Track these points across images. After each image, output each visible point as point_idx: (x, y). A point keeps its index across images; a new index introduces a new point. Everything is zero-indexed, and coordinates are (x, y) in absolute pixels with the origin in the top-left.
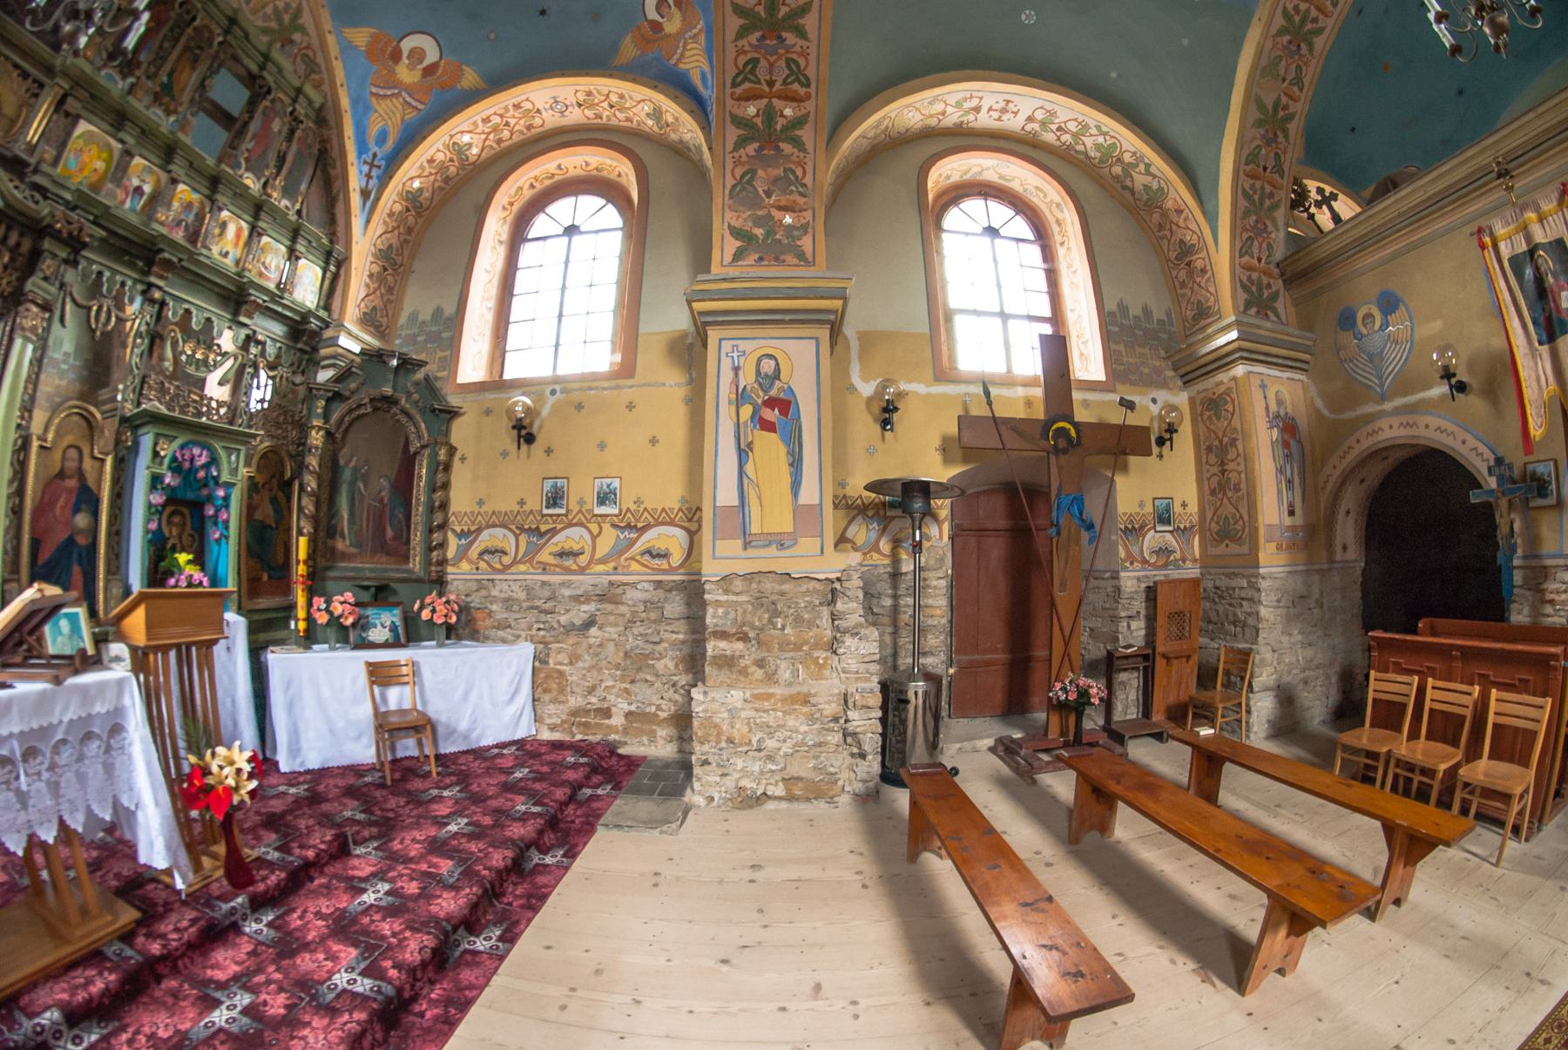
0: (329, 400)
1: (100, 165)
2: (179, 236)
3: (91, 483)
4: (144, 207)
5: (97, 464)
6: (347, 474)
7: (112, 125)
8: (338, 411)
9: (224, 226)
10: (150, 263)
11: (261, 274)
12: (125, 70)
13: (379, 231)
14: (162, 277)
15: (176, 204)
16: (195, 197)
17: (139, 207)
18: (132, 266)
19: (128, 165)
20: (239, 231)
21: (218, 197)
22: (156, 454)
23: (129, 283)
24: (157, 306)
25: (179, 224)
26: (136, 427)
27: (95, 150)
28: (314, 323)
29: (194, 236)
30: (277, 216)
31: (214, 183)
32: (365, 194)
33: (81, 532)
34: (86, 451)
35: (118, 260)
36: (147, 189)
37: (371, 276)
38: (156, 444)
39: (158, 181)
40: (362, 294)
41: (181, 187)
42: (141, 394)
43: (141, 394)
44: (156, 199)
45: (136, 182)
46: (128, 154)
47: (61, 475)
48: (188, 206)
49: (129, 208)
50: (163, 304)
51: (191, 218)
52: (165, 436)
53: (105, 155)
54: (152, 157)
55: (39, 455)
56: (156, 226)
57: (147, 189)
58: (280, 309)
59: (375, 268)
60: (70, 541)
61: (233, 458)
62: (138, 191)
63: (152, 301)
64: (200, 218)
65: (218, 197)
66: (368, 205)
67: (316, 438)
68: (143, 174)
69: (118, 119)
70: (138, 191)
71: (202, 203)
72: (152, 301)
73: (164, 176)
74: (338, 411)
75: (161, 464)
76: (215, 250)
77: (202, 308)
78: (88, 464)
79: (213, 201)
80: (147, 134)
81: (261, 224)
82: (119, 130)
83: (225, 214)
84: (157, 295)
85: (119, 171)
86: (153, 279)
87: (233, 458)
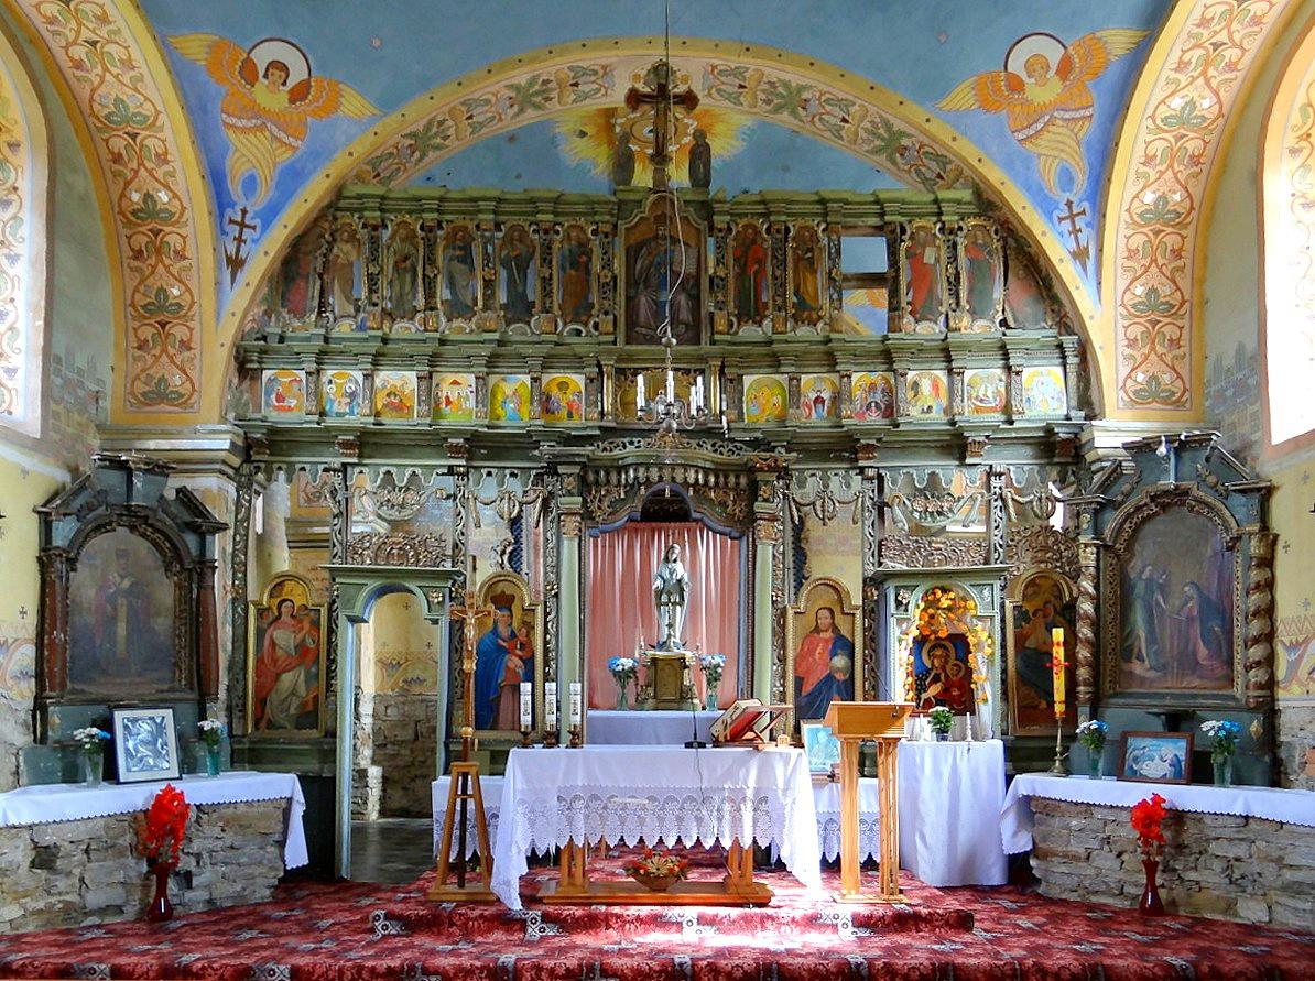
0: (1096, 513)
1: (778, 400)
2: (874, 419)
3: (845, 632)
4: (829, 413)
5: (850, 617)
6: (1140, 589)
7: (770, 366)
8: (1111, 521)
9: (916, 385)
10: (856, 452)
11: (978, 410)
12: (758, 318)
13: (1122, 285)
14: (869, 458)
15: (858, 393)
16: (874, 376)
17: (825, 414)
18: (841, 459)
19: (798, 386)
20: (936, 387)
21: (895, 366)
22: (898, 603)
23: (842, 473)
24: (875, 481)
25: (868, 407)
26: (882, 583)
27: (767, 391)
28: (1063, 434)
29: (890, 411)
30: (975, 348)
31: (887, 357)
32: (1079, 255)
33: (838, 670)
34: (837, 610)
35: (829, 460)
36: (826, 395)
37: (1132, 343)
38: (897, 595)
39: (833, 383)
40: (1124, 371)
41: (855, 377)
42: (880, 555)
43: (880, 555)
44: (837, 398)
45: (813, 396)
46: (794, 379)
47: (817, 630)
48: (872, 387)
49: (815, 419)
50: (881, 478)
51: (878, 397)
52: (905, 587)
53: (777, 390)
54: (817, 369)
55: (795, 619)
56: (844, 422)
57: (826, 395)
58: (1014, 435)
59: (1136, 331)
60: (830, 677)
61: (986, 593)
62: (819, 400)
63: (870, 479)
64: (889, 392)
65: (895, 366)
66: (1091, 264)
67: (1088, 558)
68: (814, 384)
69: (775, 362)
70: (819, 400)
71: (884, 378)
72: (870, 479)
73: (835, 377)
74: (1111, 521)
75: (906, 610)
76: (915, 412)
77: (922, 466)
78: (839, 619)
79: (894, 371)
80: (802, 360)
81: (954, 364)
82: (779, 366)
83: (911, 375)
84: (871, 472)
85: (794, 395)
86: (861, 463)
87: (986, 593)
